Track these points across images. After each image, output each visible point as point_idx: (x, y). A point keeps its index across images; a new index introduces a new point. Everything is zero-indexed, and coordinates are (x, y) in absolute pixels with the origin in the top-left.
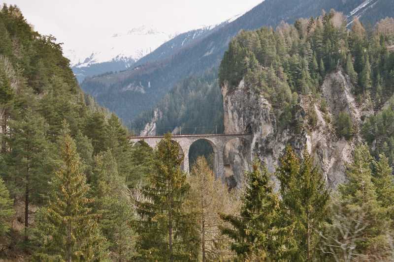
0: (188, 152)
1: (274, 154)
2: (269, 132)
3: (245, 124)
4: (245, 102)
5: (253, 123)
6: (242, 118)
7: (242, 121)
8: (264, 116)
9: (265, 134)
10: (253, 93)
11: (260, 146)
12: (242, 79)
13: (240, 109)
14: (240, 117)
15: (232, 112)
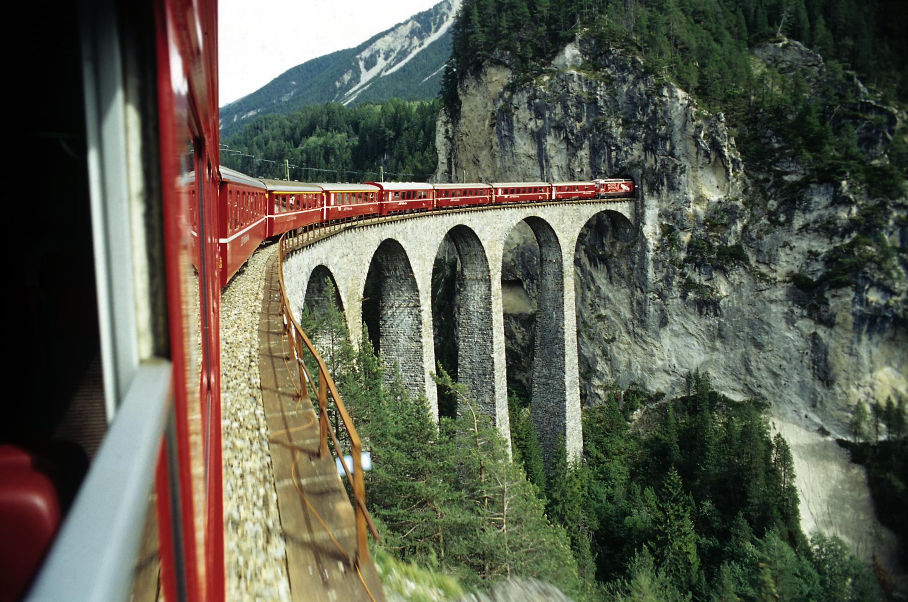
0: (500, 265)
1: (752, 261)
2: (714, 196)
3: (604, 168)
4: (601, 103)
5: (639, 164)
6: (584, 153)
7: (586, 161)
8: (704, 144)
9: (700, 199)
10: (631, 78)
11: (685, 237)
12: (571, 39)
13: (578, 125)
14: (573, 148)
15: (538, 137)
